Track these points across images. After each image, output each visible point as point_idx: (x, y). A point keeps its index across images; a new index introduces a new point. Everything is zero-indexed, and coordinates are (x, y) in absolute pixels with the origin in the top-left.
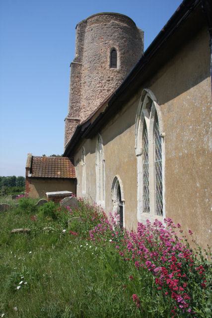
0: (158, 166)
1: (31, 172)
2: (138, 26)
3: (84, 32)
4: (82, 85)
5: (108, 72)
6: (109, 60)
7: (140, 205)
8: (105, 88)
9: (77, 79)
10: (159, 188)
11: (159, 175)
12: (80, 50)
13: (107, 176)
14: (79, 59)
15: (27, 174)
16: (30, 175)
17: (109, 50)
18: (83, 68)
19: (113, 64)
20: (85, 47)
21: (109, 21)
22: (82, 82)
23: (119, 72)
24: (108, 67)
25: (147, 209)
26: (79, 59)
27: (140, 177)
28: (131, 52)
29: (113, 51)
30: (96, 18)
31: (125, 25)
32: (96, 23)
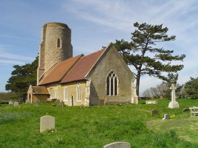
0: (80, 94)
1: (34, 92)
2: (69, 27)
3: (46, 30)
4: (45, 54)
5: (57, 49)
6: (57, 44)
7: (77, 99)
8: (56, 56)
9: (43, 51)
10: (80, 96)
11: (80, 95)
12: (44, 38)
13: (68, 94)
14: (44, 42)
15: (33, 93)
16: (34, 93)
17: (57, 40)
18: (45, 46)
19: (58, 46)
20: (47, 37)
21: (57, 27)
22: (45, 52)
23: (61, 49)
24: (57, 47)
25: (78, 100)
26: (44, 42)
27: (77, 95)
28: (66, 40)
29: (59, 40)
30: (51, 24)
31: (64, 28)
32: (51, 27)
